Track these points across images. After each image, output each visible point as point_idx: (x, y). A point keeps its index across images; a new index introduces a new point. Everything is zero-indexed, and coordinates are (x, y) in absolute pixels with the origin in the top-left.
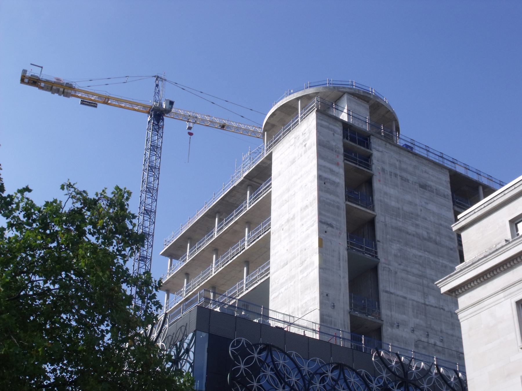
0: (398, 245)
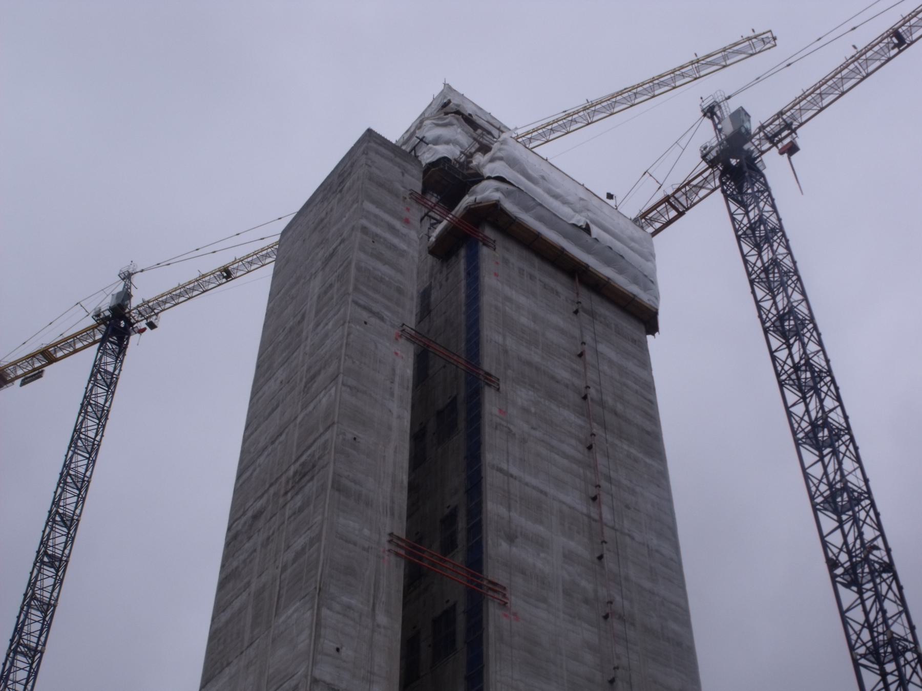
0: (531, 393)
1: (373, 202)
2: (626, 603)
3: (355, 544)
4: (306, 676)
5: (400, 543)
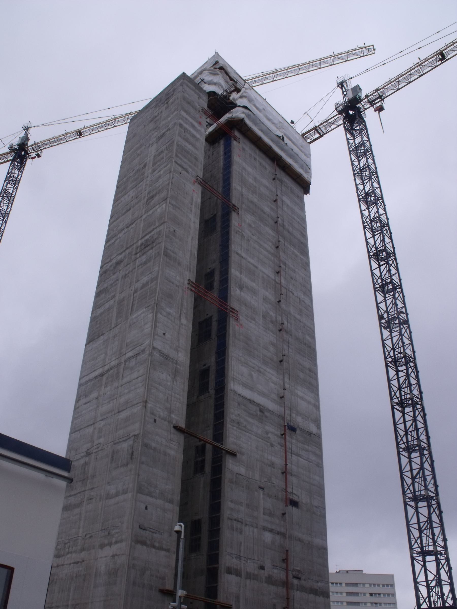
0: (252, 217)
1: (185, 111)
2: (289, 325)
3: (173, 283)
4: (149, 346)
5: (192, 284)
